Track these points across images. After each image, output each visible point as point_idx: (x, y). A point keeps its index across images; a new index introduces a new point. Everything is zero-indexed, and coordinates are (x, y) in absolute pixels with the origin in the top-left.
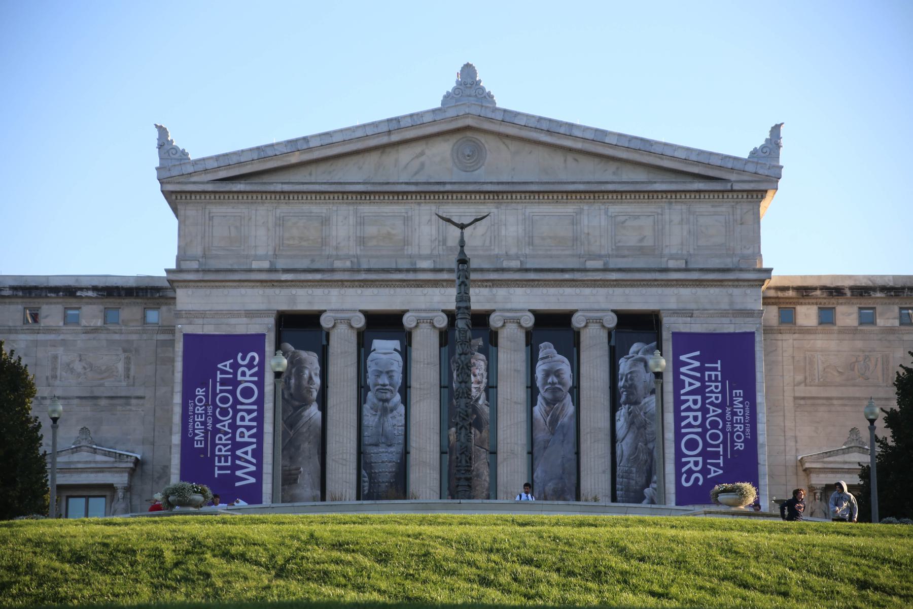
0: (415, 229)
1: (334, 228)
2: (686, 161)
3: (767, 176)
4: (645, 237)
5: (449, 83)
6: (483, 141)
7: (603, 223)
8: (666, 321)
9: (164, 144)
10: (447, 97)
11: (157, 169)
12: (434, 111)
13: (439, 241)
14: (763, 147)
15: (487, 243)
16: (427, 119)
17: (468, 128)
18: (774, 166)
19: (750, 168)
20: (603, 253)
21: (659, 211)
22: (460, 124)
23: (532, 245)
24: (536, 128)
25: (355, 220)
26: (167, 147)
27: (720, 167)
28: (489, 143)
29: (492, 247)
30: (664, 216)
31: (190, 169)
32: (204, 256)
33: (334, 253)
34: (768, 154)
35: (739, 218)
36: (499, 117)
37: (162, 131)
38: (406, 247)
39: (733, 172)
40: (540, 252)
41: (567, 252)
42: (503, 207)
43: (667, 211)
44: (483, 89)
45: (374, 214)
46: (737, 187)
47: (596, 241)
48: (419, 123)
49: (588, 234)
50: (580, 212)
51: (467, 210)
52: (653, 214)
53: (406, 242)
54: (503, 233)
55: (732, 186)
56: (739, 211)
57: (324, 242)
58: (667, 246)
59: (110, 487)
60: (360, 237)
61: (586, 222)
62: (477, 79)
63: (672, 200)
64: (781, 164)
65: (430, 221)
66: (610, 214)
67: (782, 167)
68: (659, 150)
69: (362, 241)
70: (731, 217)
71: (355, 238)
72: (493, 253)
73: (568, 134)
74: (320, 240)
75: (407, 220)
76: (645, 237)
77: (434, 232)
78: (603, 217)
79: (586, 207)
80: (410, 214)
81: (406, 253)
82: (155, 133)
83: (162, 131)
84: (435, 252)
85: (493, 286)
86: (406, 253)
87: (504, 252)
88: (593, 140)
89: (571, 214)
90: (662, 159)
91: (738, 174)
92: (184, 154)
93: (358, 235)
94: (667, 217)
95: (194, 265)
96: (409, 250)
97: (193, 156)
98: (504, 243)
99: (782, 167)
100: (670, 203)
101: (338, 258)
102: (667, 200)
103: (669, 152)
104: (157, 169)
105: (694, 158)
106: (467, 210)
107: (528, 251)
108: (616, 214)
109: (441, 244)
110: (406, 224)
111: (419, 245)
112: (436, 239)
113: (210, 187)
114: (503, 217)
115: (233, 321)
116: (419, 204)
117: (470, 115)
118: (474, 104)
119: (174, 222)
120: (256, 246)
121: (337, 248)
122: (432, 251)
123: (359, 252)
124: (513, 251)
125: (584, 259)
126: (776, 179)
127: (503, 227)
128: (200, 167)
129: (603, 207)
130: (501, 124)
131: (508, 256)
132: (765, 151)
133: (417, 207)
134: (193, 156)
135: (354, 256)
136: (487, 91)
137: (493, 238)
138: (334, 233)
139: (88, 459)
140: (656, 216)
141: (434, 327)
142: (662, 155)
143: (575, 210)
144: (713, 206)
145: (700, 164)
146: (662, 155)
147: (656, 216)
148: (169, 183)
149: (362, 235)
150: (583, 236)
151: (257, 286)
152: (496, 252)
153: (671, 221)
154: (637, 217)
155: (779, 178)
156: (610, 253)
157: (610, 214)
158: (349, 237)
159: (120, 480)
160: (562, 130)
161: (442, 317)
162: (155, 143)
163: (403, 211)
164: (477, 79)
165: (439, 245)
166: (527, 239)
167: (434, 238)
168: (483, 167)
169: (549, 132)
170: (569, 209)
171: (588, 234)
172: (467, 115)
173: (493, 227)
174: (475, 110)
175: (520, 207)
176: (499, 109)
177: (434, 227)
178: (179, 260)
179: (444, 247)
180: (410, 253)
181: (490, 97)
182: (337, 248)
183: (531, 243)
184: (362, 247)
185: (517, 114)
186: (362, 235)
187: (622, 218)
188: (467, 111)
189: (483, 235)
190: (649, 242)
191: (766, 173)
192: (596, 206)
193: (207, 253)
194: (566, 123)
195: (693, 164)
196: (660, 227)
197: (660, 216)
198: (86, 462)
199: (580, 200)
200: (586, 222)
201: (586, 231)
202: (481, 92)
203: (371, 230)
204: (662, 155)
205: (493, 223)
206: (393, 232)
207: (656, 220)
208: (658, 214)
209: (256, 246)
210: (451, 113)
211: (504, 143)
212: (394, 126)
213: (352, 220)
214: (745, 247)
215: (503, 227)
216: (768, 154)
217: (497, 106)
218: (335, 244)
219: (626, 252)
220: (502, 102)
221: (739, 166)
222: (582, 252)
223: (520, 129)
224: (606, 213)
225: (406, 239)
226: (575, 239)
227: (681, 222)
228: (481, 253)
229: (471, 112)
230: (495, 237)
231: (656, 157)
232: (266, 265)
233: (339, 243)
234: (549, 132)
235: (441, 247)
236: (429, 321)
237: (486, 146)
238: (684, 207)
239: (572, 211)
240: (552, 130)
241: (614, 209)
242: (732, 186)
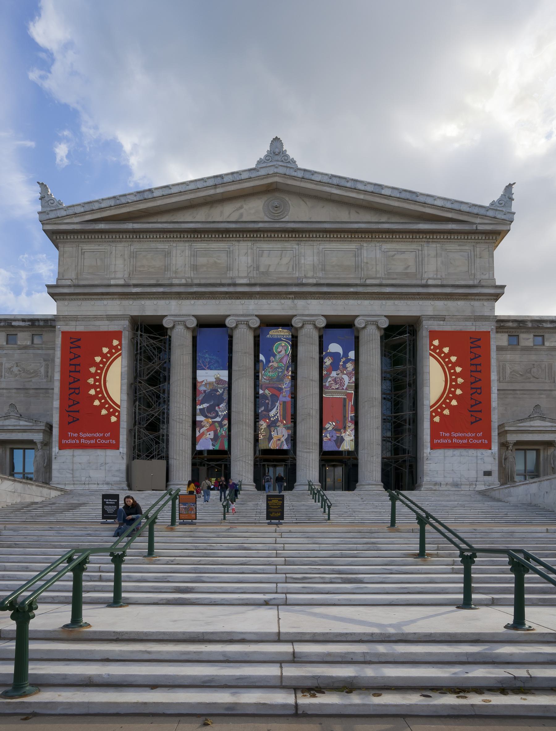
0: (236, 259)
1: (174, 258)
2: (442, 208)
3: (503, 220)
4: (409, 266)
5: (263, 150)
6: (287, 199)
7: (378, 256)
12: (250, 170)
13: (254, 268)
14: (499, 200)
15: (290, 270)
16: (245, 176)
18: (509, 212)
19: (491, 213)
20: (378, 276)
21: (420, 248)
23: (324, 270)
24: (328, 183)
25: (190, 252)
27: (468, 213)
29: (294, 272)
30: (423, 252)
32: (77, 279)
33: (174, 276)
34: (503, 205)
35: (478, 253)
36: (300, 174)
38: (228, 272)
39: (477, 217)
40: (331, 276)
41: (352, 276)
42: (302, 244)
43: (426, 248)
44: (287, 156)
45: (204, 249)
46: (480, 227)
47: (373, 268)
48: (238, 179)
49: (367, 263)
50: (361, 247)
51: (275, 246)
52: (415, 250)
53: (229, 268)
54: (303, 261)
55: (476, 227)
56: (478, 249)
57: (167, 268)
58: (426, 272)
59: (31, 442)
60: (194, 265)
61: (365, 255)
62: (284, 150)
63: (429, 240)
64: (513, 210)
65: (247, 253)
66: (383, 250)
67: (514, 213)
68: (421, 199)
69: (195, 267)
70: (472, 253)
71: (189, 265)
72: (294, 276)
73: (353, 187)
74: (164, 267)
75: (229, 253)
76: (409, 266)
77: (250, 261)
78: (378, 251)
79: (365, 245)
80: (231, 249)
81: (228, 276)
84: (250, 275)
85: (295, 298)
86: (228, 276)
87: (303, 275)
88: (372, 192)
89: (354, 250)
90: (424, 207)
91: (483, 218)
93: (192, 263)
94: (426, 252)
95: (69, 282)
96: (230, 274)
98: (303, 269)
99: (514, 213)
100: (428, 242)
101: (176, 278)
102: (426, 240)
103: (429, 201)
105: (449, 205)
106: (275, 246)
107: (320, 274)
108: (387, 250)
109: (255, 269)
110: (229, 256)
111: (238, 270)
112: (251, 266)
114: (303, 251)
116: (239, 241)
117: (278, 174)
118: (281, 166)
120: (115, 272)
121: (176, 272)
122: (248, 275)
123: (192, 276)
124: (310, 274)
125: (364, 280)
126: (510, 223)
127: (303, 258)
129: (378, 245)
130: (301, 181)
131: (306, 277)
132: (501, 202)
133: (237, 244)
135: (189, 278)
137: (294, 265)
138: (174, 262)
139: (15, 424)
140: (417, 252)
142: (424, 203)
143: (357, 247)
144: (459, 245)
145: (453, 211)
146: (425, 203)
147: (417, 252)
149: (195, 264)
150: (363, 264)
151: (116, 299)
152: (297, 276)
153: (429, 255)
154: (404, 252)
155: (512, 222)
156: (383, 276)
157: (383, 250)
158: (185, 265)
159: (38, 437)
160: (349, 185)
163: (227, 247)
164: (284, 150)
165: (253, 270)
166: (320, 266)
167: (249, 265)
168: (287, 217)
169: (338, 186)
170: (353, 246)
171: (367, 263)
172: (275, 174)
173: (294, 258)
174: (281, 170)
175: (315, 243)
176: (300, 169)
177: (250, 258)
178: (58, 280)
179: (258, 272)
180: (231, 276)
182: (176, 272)
183: (323, 269)
184: (195, 272)
185: (313, 173)
186: (195, 264)
187: (392, 253)
188: (276, 170)
189: (287, 264)
190: (412, 270)
191: (503, 217)
192: (373, 244)
193: (79, 277)
194: (352, 180)
195: (446, 211)
196: (420, 259)
197: (420, 252)
198: (14, 426)
199: (361, 239)
200: (365, 255)
201: (365, 261)
202: (286, 158)
203: (202, 260)
204: (424, 204)
205: (294, 256)
206: (219, 261)
207: (417, 255)
208: (419, 250)
209: (115, 272)
210: (263, 172)
211: (303, 200)
212: (219, 181)
213: (187, 253)
214: (483, 274)
215: (303, 258)
216: (503, 205)
217: (299, 166)
218: (174, 269)
219: (395, 277)
220: (301, 165)
221: (482, 212)
222: (363, 276)
223: (316, 184)
224: (380, 249)
225: (229, 266)
226: (357, 267)
227: (436, 256)
228: (286, 276)
229: (278, 172)
230: (296, 265)
231: (420, 205)
232: (121, 282)
233: (177, 269)
234: (338, 186)
235: (255, 272)
237: (290, 202)
238: (438, 245)
239: (354, 247)
240: (340, 185)
241: (387, 246)
242: (476, 227)
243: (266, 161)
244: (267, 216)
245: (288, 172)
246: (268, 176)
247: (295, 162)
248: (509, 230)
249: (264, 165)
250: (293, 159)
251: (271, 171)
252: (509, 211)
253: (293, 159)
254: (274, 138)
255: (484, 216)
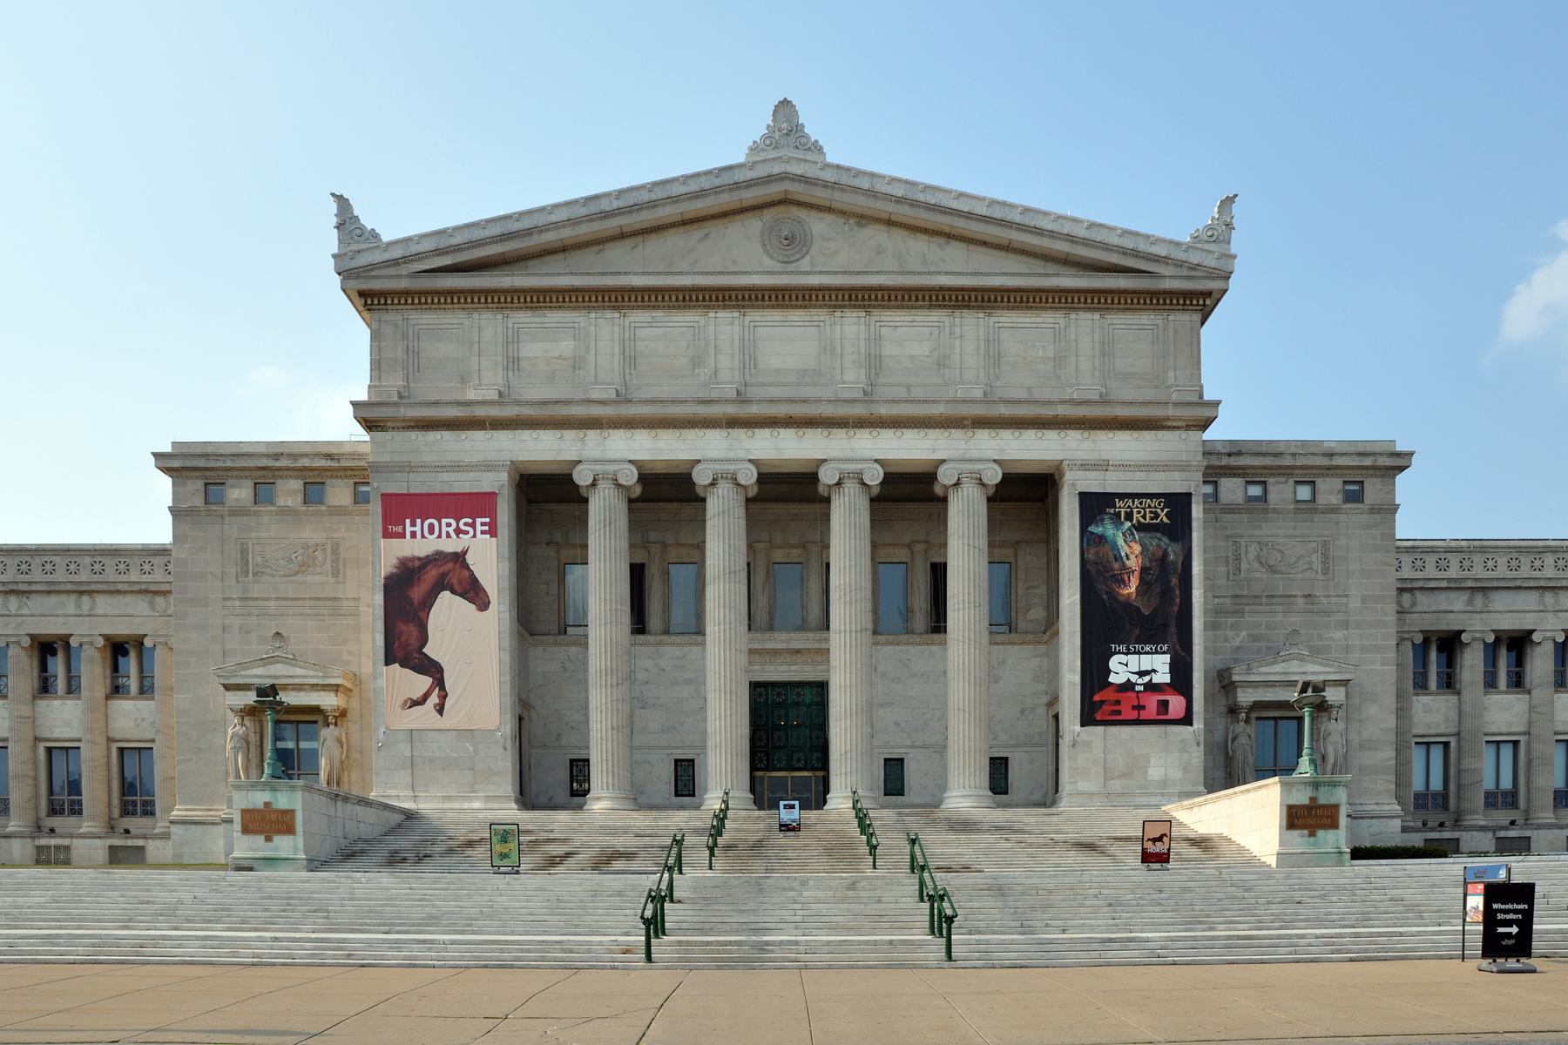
8: (1069, 476)
9: (346, 221)
10: (754, 149)
11: (334, 256)
17: (785, 201)
19: (1194, 258)
22: (775, 190)
26: (349, 227)
28: (818, 225)
31: (378, 257)
36: (829, 176)
37: (342, 202)
64: (1233, 251)
67: (1234, 257)
82: (333, 207)
83: (342, 202)
92: (374, 235)
97: (386, 237)
99: (1234, 257)
104: (334, 256)
113: (404, 284)
115: (445, 476)
119: (366, 333)
128: (397, 253)
134: (386, 238)
136: (813, 140)
141: (738, 484)
148: (349, 278)
161: (752, 476)
162: (334, 221)
174: (797, 169)
181: (817, 148)
191: (1213, 263)
210: (760, 172)
221: (1179, 255)
236: (729, 476)
243: (766, 148)
244: (770, 256)
245: (812, 171)
246: (769, 179)
247: (820, 150)
248: (1226, 291)
249: (763, 156)
250: (816, 141)
251: (777, 169)
252: (1226, 252)
253: (816, 141)
254: (782, 99)
255: (1180, 264)
